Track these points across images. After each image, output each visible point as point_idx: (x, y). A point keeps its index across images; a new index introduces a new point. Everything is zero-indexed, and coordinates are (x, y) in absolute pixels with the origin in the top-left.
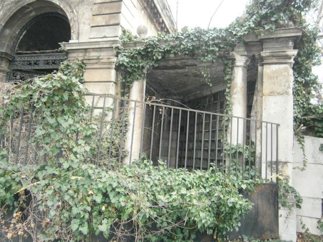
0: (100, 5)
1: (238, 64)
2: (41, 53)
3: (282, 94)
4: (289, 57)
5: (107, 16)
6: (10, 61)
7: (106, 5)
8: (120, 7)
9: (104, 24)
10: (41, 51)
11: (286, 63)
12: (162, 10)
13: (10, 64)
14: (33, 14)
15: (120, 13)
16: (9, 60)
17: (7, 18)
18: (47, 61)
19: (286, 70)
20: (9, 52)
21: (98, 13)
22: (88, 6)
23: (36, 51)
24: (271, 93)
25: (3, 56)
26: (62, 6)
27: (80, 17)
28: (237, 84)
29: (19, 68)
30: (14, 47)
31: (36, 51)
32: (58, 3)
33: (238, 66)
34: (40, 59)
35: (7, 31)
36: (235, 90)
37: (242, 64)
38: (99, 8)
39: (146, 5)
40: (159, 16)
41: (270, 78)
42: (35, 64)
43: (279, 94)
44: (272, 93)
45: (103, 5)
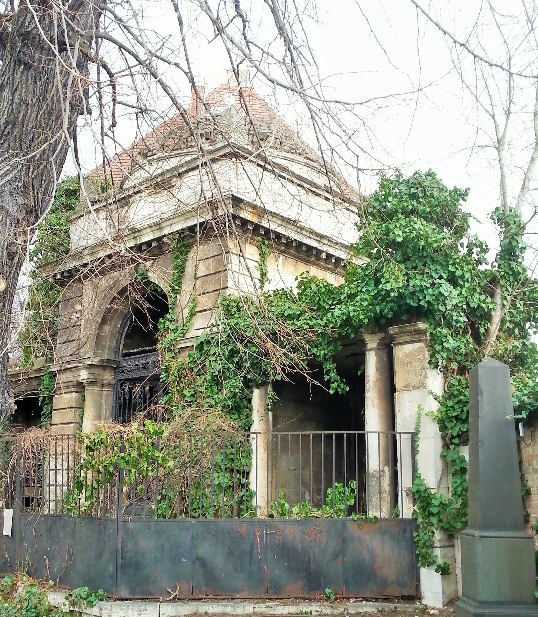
1: (369, 346)
3: (418, 388)
6: (115, 368)
11: (420, 341)
15: (227, 288)
16: (113, 367)
19: (421, 350)
23: (145, 348)
24: (406, 387)
25: (105, 364)
28: (369, 376)
30: (118, 347)
33: (369, 350)
35: (107, 328)
37: (375, 345)
38: (203, 283)
41: (404, 364)
44: (407, 387)
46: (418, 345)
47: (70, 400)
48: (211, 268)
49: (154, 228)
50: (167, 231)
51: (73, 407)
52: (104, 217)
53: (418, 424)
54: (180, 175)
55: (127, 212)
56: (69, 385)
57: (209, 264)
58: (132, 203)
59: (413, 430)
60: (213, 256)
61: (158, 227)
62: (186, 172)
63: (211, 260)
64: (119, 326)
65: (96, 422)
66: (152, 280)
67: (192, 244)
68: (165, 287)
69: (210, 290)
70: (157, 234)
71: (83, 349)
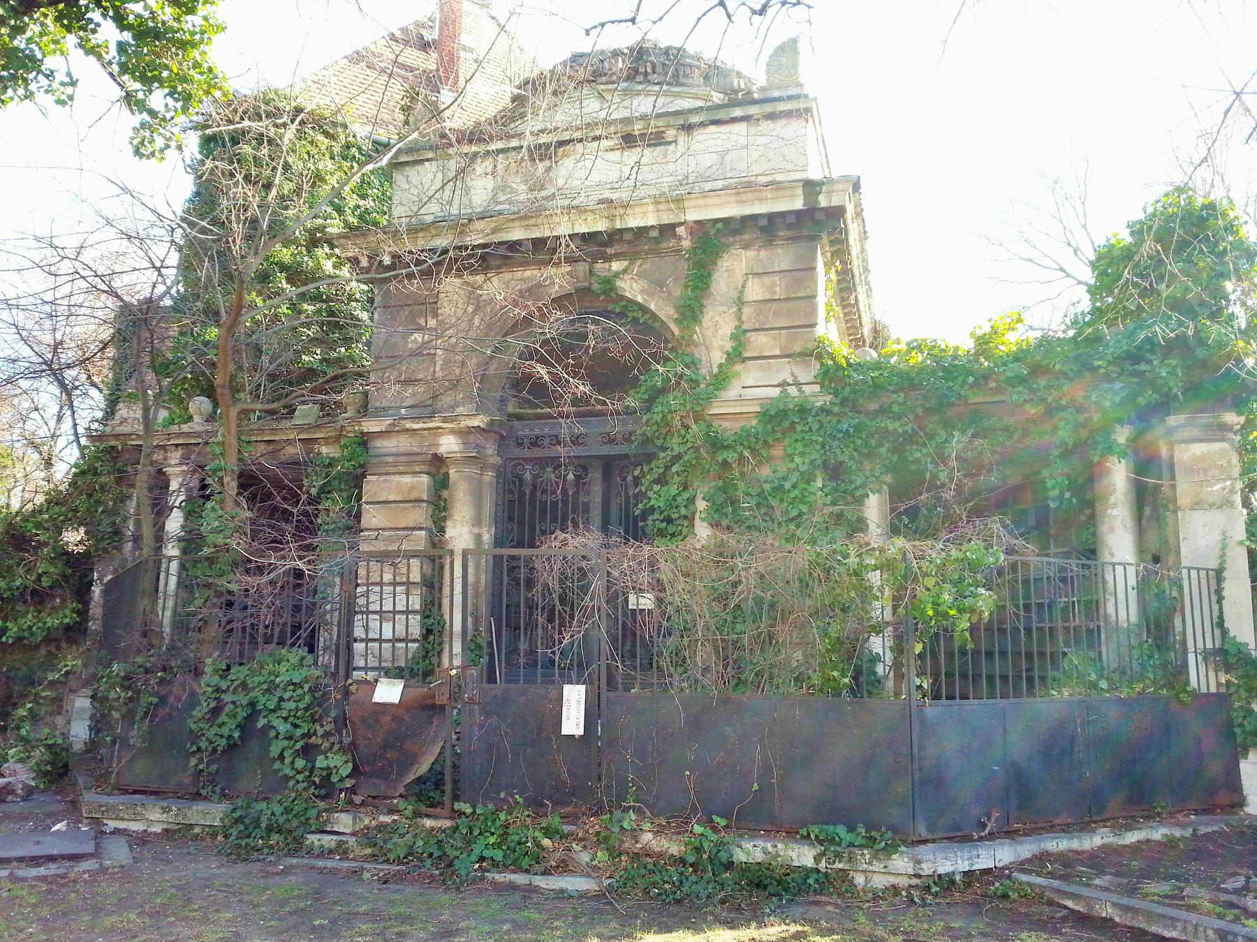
3: (1220, 507)
4: (1228, 428)
5: (783, 332)
7: (775, 306)
9: (778, 352)
11: (1223, 440)
21: (757, 326)
24: (1196, 504)
26: (652, 307)
27: (709, 333)
32: (640, 299)
36: (1113, 499)
43: (1211, 505)
44: (1197, 505)
46: (1217, 446)
47: (412, 488)
48: (778, 289)
50: (692, 216)
51: (422, 501)
52: (489, 170)
53: (1223, 556)
54: (688, 128)
56: (408, 461)
57: (773, 284)
59: (1214, 564)
60: (780, 272)
65: (476, 530)
68: (663, 309)
70: (667, 219)
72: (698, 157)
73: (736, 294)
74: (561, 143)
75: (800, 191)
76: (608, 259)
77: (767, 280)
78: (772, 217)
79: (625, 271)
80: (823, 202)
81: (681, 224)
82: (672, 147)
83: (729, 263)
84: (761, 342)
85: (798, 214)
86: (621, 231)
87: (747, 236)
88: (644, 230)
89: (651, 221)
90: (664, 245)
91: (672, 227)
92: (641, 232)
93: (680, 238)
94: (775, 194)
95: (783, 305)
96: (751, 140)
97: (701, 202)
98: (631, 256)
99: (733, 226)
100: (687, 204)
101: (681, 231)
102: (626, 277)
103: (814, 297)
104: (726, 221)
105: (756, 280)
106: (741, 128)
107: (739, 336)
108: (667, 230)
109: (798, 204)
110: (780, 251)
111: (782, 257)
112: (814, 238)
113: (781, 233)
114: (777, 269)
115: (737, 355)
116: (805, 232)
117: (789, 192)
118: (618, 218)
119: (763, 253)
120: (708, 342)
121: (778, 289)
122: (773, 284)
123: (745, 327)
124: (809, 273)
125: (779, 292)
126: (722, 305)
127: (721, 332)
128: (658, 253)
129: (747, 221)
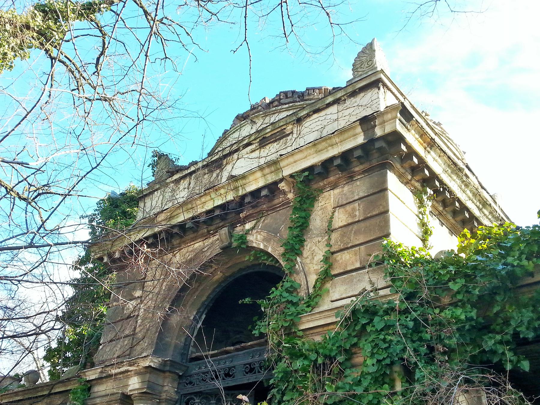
0: (345, 229)
2: (237, 350)
5: (362, 247)
7: (355, 227)
8: (386, 223)
10: (238, 346)
12: (480, 210)
13: (179, 384)
14: (219, 275)
17: (173, 293)
18: (250, 364)
20: (178, 359)
21: (342, 247)
22: (320, 239)
26: (270, 250)
27: (308, 261)
29: (197, 390)
31: (228, 348)
32: (262, 247)
34: (235, 363)
38: (343, 236)
39: (441, 209)
40: (476, 224)
42: (227, 375)
45: (350, 227)
48: (357, 213)
49: (267, 171)
50: (287, 172)
55: (218, 176)
57: (354, 210)
58: (226, 164)
60: (359, 199)
61: (273, 169)
62: (308, 115)
63: (356, 205)
64: (192, 318)
66: (254, 245)
67: (322, 189)
68: (275, 250)
69: (358, 243)
70: (271, 178)
71: (138, 348)
72: (305, 138)
73: (325, 225)
74: (225, 156)
75: (359, 129)
76: (243, 222)
77: (349, 208)
78: (346, 156)
79: (253, 228)
80: (379, 132)
81: (281, 180)
82: (290, 137)
83: (323, 203)
84: (347, 260)
85: (361, 147)
86: (243, 197)
87: (332, 179)
88: (259, 190)
89: (261, 183)
90: (276, 201)
91: (275, 183)
92: (255, 194)
93: (284, 193)
94: (342, 138)
95: (362, 225)
96: (340, 114)
97: (291, 160)
98: (258, 216)
99: (317, 171)
100: (282, 164)
101: (282, 186)
102: (254, 231)
103: (387, 211)
104: (311, 169)
105: (341, 210)
106: (334, 109)
107: (328, 259)
108: (273, 188)
109: (360, 140)
110: (358, 183)
111: (360, 187)
112: (384, 166)
113: (357, 169)
114: (356, 197)
115: (326, 276)
116: (375, 163)
117: (351, 133)
118: (240, 188)
119: (346, 188)
120: (306, 269)
121: (357, 213)
122: (354, 210)
123: (332, 250)
124: (382, 194)
125: (359, 215)
126: (318, 236)
127: (316, 259)
128: (273, 209)
129: (327, 164)
